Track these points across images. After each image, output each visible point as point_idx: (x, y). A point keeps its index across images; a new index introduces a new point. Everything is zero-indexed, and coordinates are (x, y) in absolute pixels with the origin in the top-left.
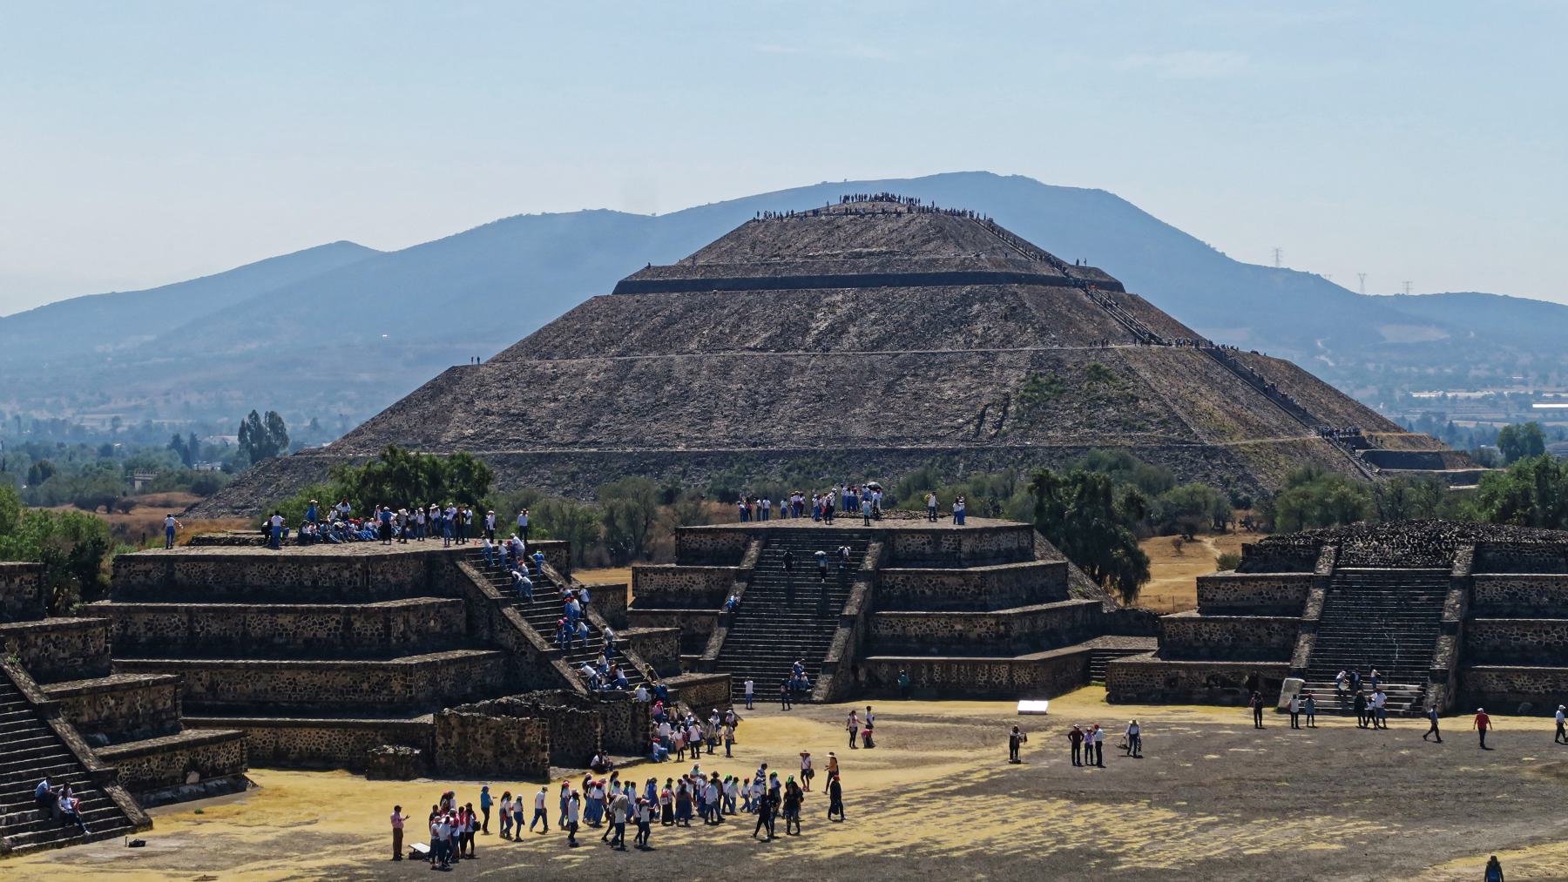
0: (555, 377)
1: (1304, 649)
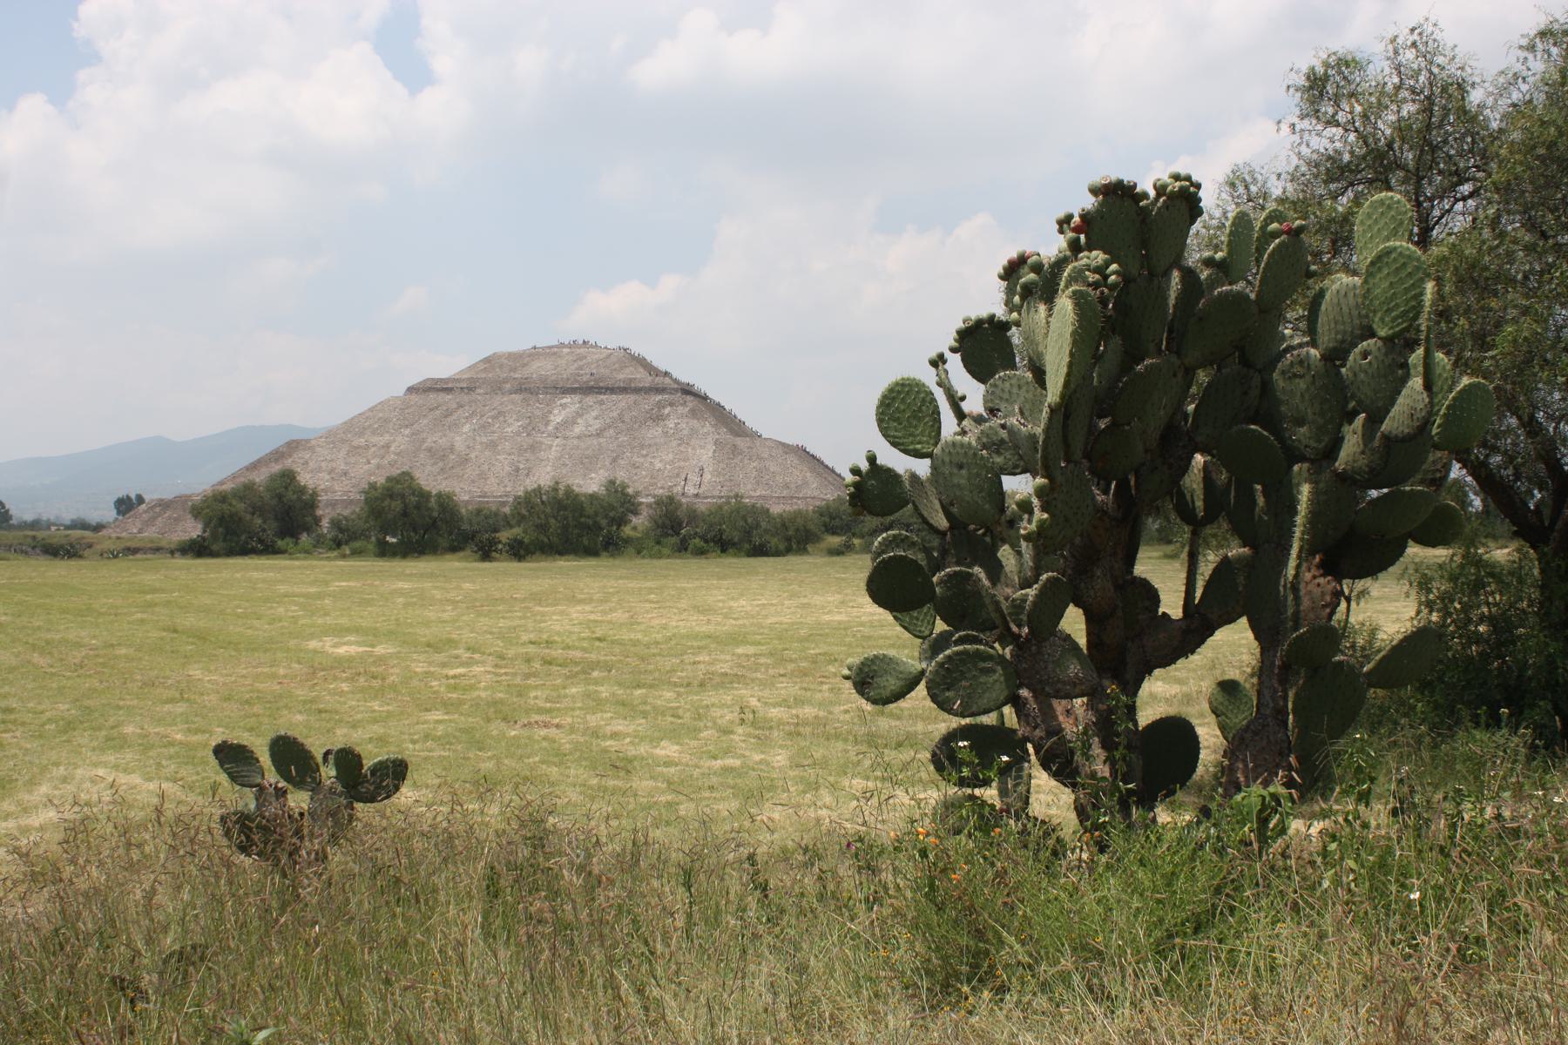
0: (367, 447)
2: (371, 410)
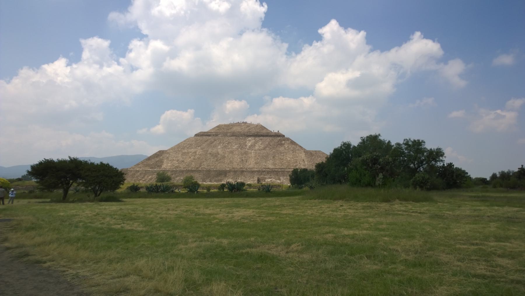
0: (188, 153)
2: (185, 141)
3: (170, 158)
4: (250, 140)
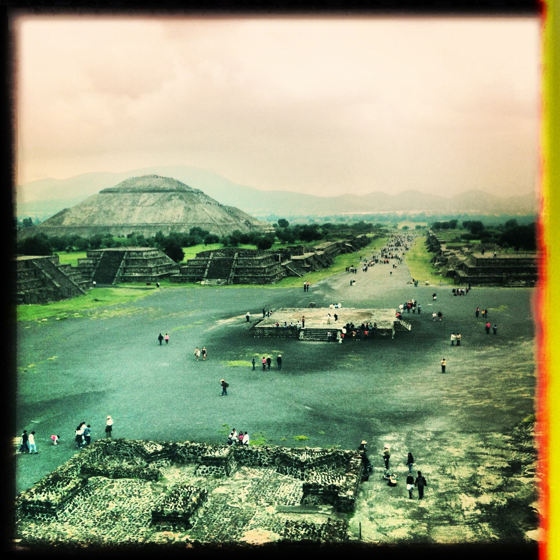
1: (206, 273)
3: (71, 216)
4: (144, 197)
